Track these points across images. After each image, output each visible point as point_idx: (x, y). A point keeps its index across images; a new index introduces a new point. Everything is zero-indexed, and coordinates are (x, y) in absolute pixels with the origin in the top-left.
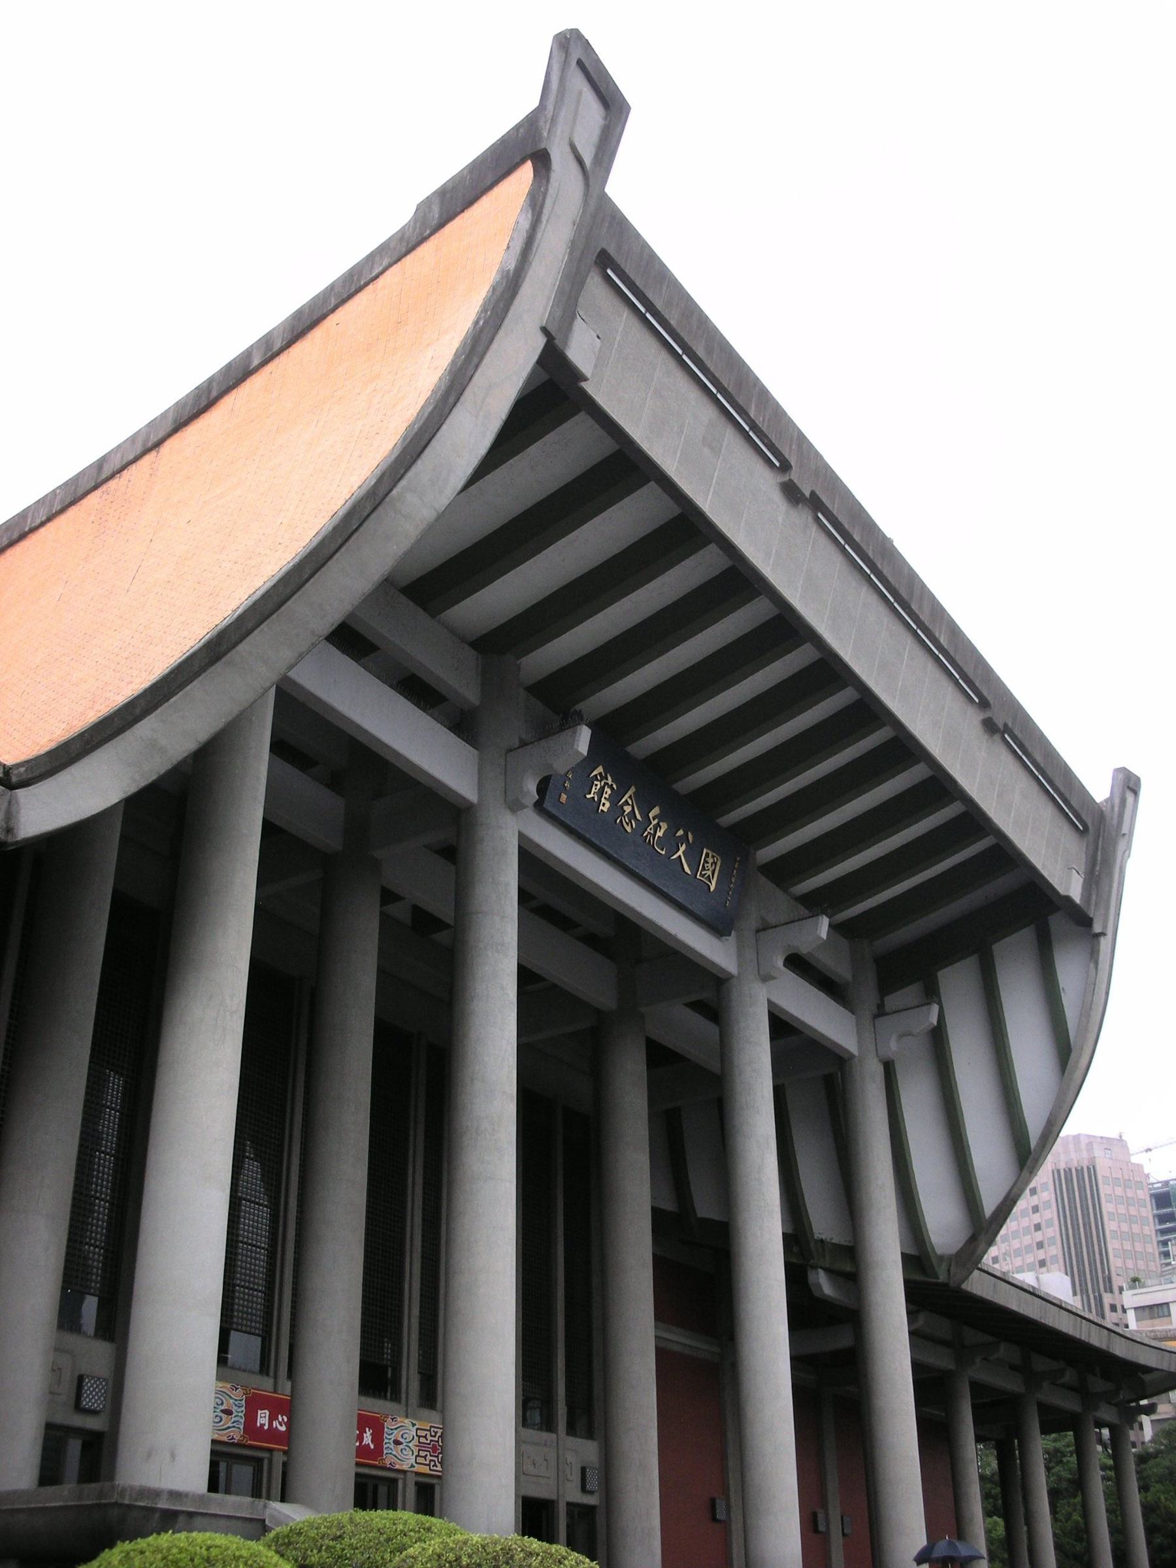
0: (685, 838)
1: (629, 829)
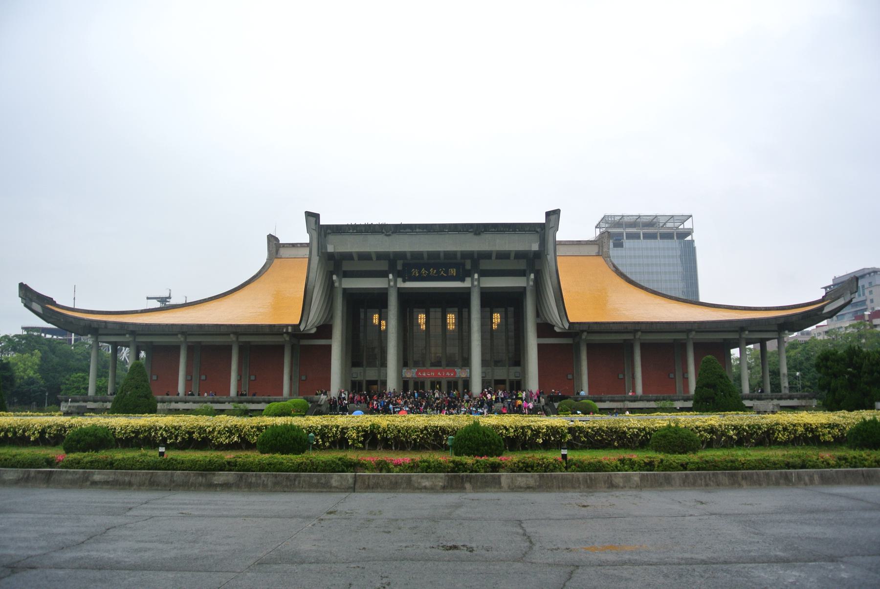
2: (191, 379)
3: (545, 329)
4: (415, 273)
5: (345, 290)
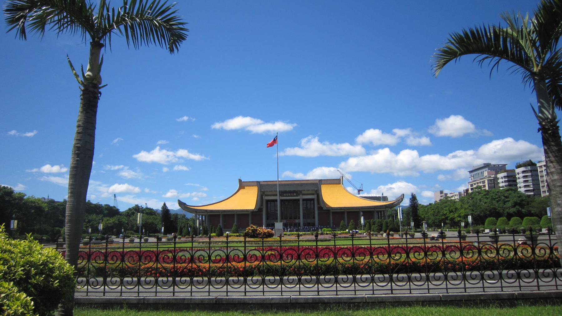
3: (320, 208)
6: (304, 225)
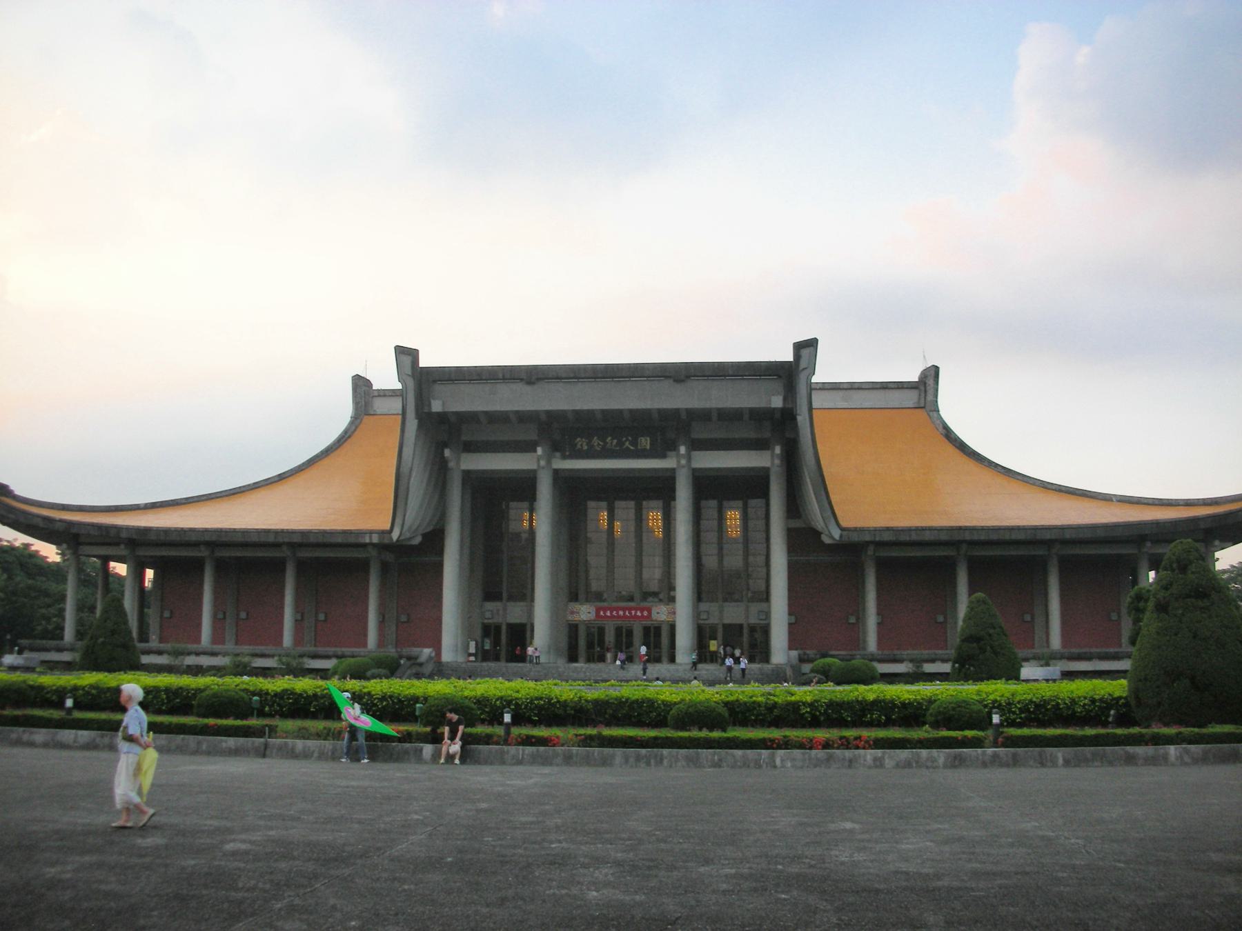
0: (627, 440)
1: (599, 449)
2: (225, 618)
4: (581, 445)
5: (467, 474)
6: (702, 635)
